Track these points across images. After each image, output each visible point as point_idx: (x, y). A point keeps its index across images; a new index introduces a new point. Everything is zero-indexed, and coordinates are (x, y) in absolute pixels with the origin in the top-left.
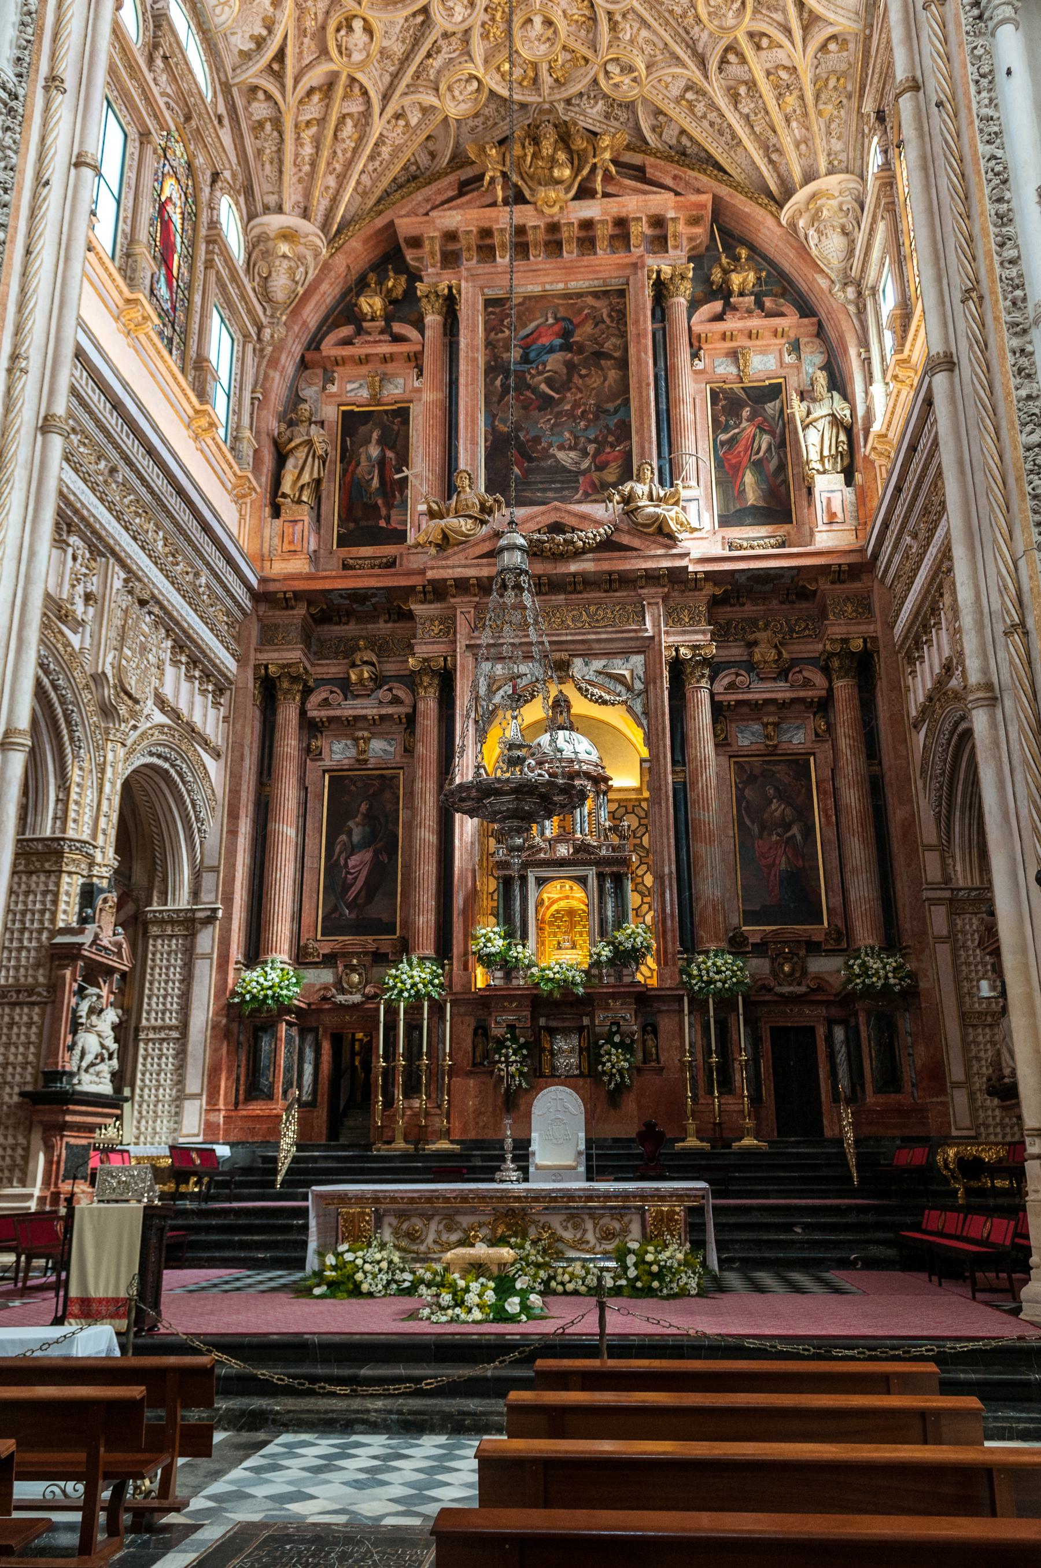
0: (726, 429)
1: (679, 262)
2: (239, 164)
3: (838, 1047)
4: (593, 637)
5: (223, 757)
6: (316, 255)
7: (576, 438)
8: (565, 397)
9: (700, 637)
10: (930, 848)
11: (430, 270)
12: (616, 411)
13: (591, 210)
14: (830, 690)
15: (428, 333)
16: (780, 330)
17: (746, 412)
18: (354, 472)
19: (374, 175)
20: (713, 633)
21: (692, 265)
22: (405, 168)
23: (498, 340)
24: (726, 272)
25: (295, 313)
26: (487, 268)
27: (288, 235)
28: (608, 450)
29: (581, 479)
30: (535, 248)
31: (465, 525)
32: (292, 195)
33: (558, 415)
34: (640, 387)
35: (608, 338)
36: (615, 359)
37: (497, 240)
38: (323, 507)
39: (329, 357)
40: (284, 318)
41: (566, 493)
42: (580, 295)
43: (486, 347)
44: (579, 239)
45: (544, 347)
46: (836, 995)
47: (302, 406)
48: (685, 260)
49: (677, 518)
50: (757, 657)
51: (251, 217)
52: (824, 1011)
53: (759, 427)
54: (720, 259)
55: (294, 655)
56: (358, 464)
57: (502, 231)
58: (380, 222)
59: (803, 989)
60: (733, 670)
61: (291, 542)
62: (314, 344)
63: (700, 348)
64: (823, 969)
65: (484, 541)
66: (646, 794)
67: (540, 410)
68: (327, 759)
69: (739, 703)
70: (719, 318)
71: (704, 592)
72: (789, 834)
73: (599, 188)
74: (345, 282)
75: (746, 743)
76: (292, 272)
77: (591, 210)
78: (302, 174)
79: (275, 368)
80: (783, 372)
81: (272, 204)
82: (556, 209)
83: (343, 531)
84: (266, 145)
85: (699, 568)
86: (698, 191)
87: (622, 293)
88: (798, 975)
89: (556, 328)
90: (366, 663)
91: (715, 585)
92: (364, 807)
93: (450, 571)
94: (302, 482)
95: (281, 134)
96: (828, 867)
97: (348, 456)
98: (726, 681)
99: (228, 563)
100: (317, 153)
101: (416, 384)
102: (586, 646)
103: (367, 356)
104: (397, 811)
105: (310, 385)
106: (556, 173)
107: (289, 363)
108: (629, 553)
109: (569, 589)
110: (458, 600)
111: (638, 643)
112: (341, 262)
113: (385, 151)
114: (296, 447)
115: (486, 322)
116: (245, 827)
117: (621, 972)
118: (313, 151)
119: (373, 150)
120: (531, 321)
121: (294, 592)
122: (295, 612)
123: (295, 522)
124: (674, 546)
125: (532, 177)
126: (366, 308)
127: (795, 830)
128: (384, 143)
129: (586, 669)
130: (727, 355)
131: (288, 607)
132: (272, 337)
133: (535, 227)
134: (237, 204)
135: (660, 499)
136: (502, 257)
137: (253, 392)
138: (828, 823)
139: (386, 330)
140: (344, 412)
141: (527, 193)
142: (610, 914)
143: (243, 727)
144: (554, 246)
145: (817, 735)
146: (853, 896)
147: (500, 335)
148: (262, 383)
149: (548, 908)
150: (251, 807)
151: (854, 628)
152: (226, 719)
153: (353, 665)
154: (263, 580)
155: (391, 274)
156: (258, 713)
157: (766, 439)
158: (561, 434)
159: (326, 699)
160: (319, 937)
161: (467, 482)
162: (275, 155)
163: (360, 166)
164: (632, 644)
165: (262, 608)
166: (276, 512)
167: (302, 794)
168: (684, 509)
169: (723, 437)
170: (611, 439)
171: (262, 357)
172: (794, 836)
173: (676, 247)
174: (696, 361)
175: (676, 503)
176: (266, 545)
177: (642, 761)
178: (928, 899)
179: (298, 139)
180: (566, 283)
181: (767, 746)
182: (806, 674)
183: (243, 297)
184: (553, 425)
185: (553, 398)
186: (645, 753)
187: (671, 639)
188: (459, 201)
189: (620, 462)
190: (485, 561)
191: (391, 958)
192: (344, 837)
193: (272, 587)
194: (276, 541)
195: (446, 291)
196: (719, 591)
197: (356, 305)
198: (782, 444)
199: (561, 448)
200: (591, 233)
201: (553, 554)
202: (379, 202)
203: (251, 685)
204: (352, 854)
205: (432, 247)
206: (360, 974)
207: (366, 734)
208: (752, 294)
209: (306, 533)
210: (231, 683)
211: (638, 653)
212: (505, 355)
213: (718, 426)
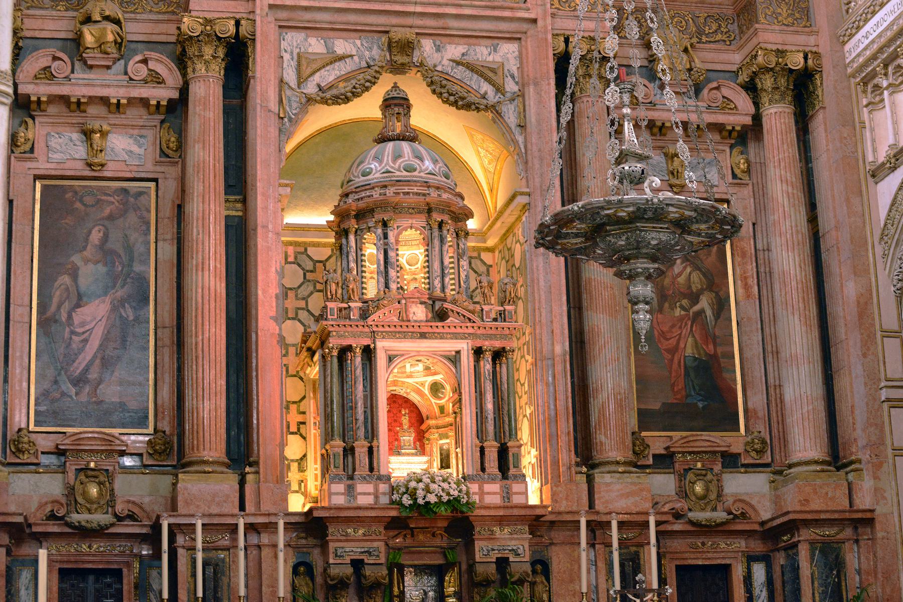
3: (756, 592)
10: (888, 334)
14: (757, 118)
46: (763, 523)
52: (741, 544)
59: (720, 516)
64: (741, 490)
66: (490, 243)
68: (42, 158)
72: (696, 308)
88: (713, 496)
90: (107, 18)
92: (96, 236)
96: (748, 354)
102: (440, 23)
104: (149, 243)
111: (513, 26)
127: (704, 303)
129: (437, 56)
138: (748, 296)
142: (489, 406)
145: (734, 176)
146: (789, 394)
151: (790, 38)
153: (88, 20)
159: (47, 69)
164: (504, 26)
172: (702, 311)
178: (888, 400)
182: (725, 92)
192: (65, 279)
204: (78, 306)
206: (100, 484)
207: (106, 127)
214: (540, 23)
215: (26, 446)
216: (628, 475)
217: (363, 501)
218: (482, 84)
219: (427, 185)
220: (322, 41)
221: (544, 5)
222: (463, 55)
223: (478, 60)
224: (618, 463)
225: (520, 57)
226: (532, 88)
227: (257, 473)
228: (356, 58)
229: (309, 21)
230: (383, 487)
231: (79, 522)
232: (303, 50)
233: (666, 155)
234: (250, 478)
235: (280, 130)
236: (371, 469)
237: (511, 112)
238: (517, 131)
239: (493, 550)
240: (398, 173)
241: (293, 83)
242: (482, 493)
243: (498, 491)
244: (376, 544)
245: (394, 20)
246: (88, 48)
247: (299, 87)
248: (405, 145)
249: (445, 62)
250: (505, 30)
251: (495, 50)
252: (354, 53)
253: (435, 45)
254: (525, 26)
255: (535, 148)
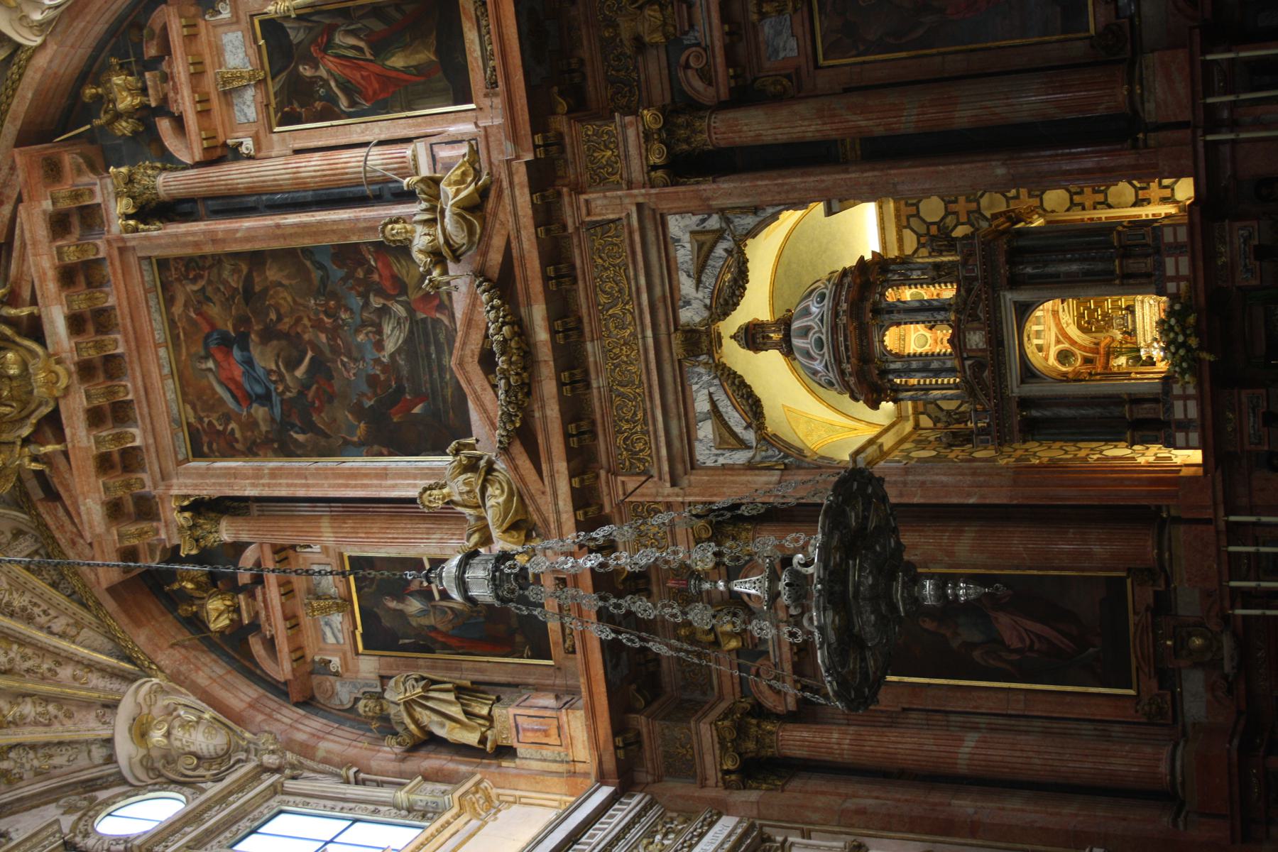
0: (332, 99)
1: (110, 188)
2: (56, 800)
4: (645, 297)
5: (861, 839)
6: (162, 690)
7: (364, 324)
8: (310, 342)
9: (631, 133)
11: (163, 536)
12: (321, 267)
13: (56, 320)
15: (244, 537)
16: (185, 31)
17: (306, 71)
18: (445, 634)
19: (52, 612)
20: (624, 114)
21: (112, 169)
22: (36, 571)
23: (245, 438)
24: (118, 116)
25: (239, 719)
26: (151, 460)
27: (140, 731)
28: (376, 277)
29: (421, 315)
30: (115, 393)
31: (496, 497)
32: (89, 726)
33: (335, 351)
34: (284, 237)
35: (225, 283)
36: (250, 272)
37: (113, 448)
38: (497, 678)
39: (294, 670)
40: (247, 735)
41: (442, 337)
42: (172, 323)
43: (255, 455)
44: (98, 332)
45: (245, 373)
47: (361, 710)
48: (108, 181)
49: (457, 183)
50: (658, 38)
51: (124, 781)
53: (324, 51)
54: (101, 127)
55: (706, 733)
56: (434, 628)
57: (98, 442)
58: (110, 605)
60: (681, 74)
61: (546, 733)
62: (279, 690)
63: (225, 145)
65: (516, 468)
67: (332, 377)
69: (731, 60)
70: (179, 123)
71: (565, 129)
73: (25, 311)
74: (195, 648)
75: (793, 43)
76: (185, 725)
77: (56, 320)
78: (60, 714)
79: (314, 748)
80: (244, 19)
81: (104, 752)
82: (58, 368)
83: (527, 651)
84: (28, 766)
85: (528, 143)
86: (13, 168)
87: (163, 264)
89: (219, 356)
91: (554, 113)
93: (564, 517)
94: (462, 717)
95: (12, 747)
97: (425, 643)
98: (698, 84)
99: (576, 842)
100: (31, 695)
101: (317, 548)
102: (660, 305)
103: (286, 618)
105: (334, 693)
106: (13, 371)
107: (308, 726)
108: (515, 253)
109: (574, 338)
110: (606, 501)
111: (649, 226)
112: (165, 658)
113: (19, 601)
114: (416, 722)
115: (224, 456)
116: (965, 806)
117: (1170, 245)
118: (28, 700)
119: (20, 618)
120: (213, 389)
121: (616, 732)
122: (644, 730)
123: (517, 726)
124: (500, 181)
125: (25, 404)
126: (224, 622)
128: (9, 604)
129: (696, 304)
130: (230, 105)
131: (638, 741)
132: (273, 752)
133: (88, 397)
134: (107, 803)
135: (432, 209)
136: (133, 438)
137: (347, 782)
139: (249, 590)
140: (365, 647)
141: (45, 410)
142: (1075, 267)
143: (816, 810)
144: (112, 366)
147: (238, 435)
148: (337, 767)
149: (1073, 343)
150: (935, 798)
152: (806, 834)
153: (716, 643)
154: (602, 779)
155: (176, 586)
156: (796, 784)
157: (339, 39)
158: (360, 347)
160: (1131, 692)
161: (434, 492)
162: (41, 752)
163: (41, 636)
164: (651, 236)
165: (643, 777)
166: (505, 752)
167: (913, 715)
168: (447, 168)
169: (343, 103)
170: (360, 273)
171: (301, 766)
173: (92, 193)
174: (243, 150)
175: (434, 182)
176: (554, 767)
177: (830, 212)
179: (14, 723)
180: (157, 346)
181: (795, 10)
183: (222, 799)
184: (350, 358)
185: (312, 359)
186: (819, 208)
187: (637, 173)
188: (68, 502)
189: (392, 260)
190: (544, 467)
191: (1162, 587)
192: (976, 654)
193: (610, 764)
194: (547, 752)
195: (187, 514)
196: (563, 106)
197: (221, 632)
198: (345, 13)
199: (379, 345)
200: (88, 315)
201: (524, 369)
202: (84, 605)
203: (753, 795)
205: (132, 536)
206: (1190, 635)
208: (141, 75)
209: (532, 712)
210: (752, 827)
211: (664, 224)
212: (264, 428)
213: (329, 113)
214: (640, 200)
215: (1154, 707)
216: (1145, 82)
217: (1193, 412)
218: (717, 255)
219: (834, 328)
220: (700, 424)
221: (620, 197)
222: (689, 276)
223: (691, 260)
224: (1131, 91)
225: (681, 213)
226: (711, 203)
227: (1168, 506)
228: (712, 389)
229: (682, 440)
230: (1177, 389)
231: (1233, 668)
232: (712, 444)
233: (760, 20)
234: (1173, 512)
235: (799, 467)
236: (1155, 400)
237: (742, 222)
238: (763, 215)
239: (1246, 265)
240: (826, 356)
241: (749, 454)
242: (1177, 278)
243: (1173, 259)
244: (1244, 399)
245: (666, 354)
246: (743, 645)
247: (750, 448)
248: (797, 342)
249: (700, 295)
250: (654, 233)
251: (678, 241)
252: (706, 392)
253: (684, 307)
254: (647, 212)
255: (778, 197)
